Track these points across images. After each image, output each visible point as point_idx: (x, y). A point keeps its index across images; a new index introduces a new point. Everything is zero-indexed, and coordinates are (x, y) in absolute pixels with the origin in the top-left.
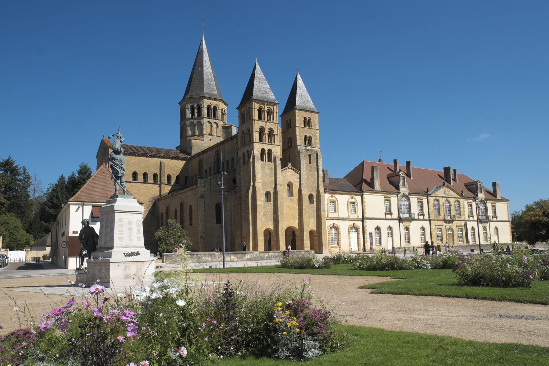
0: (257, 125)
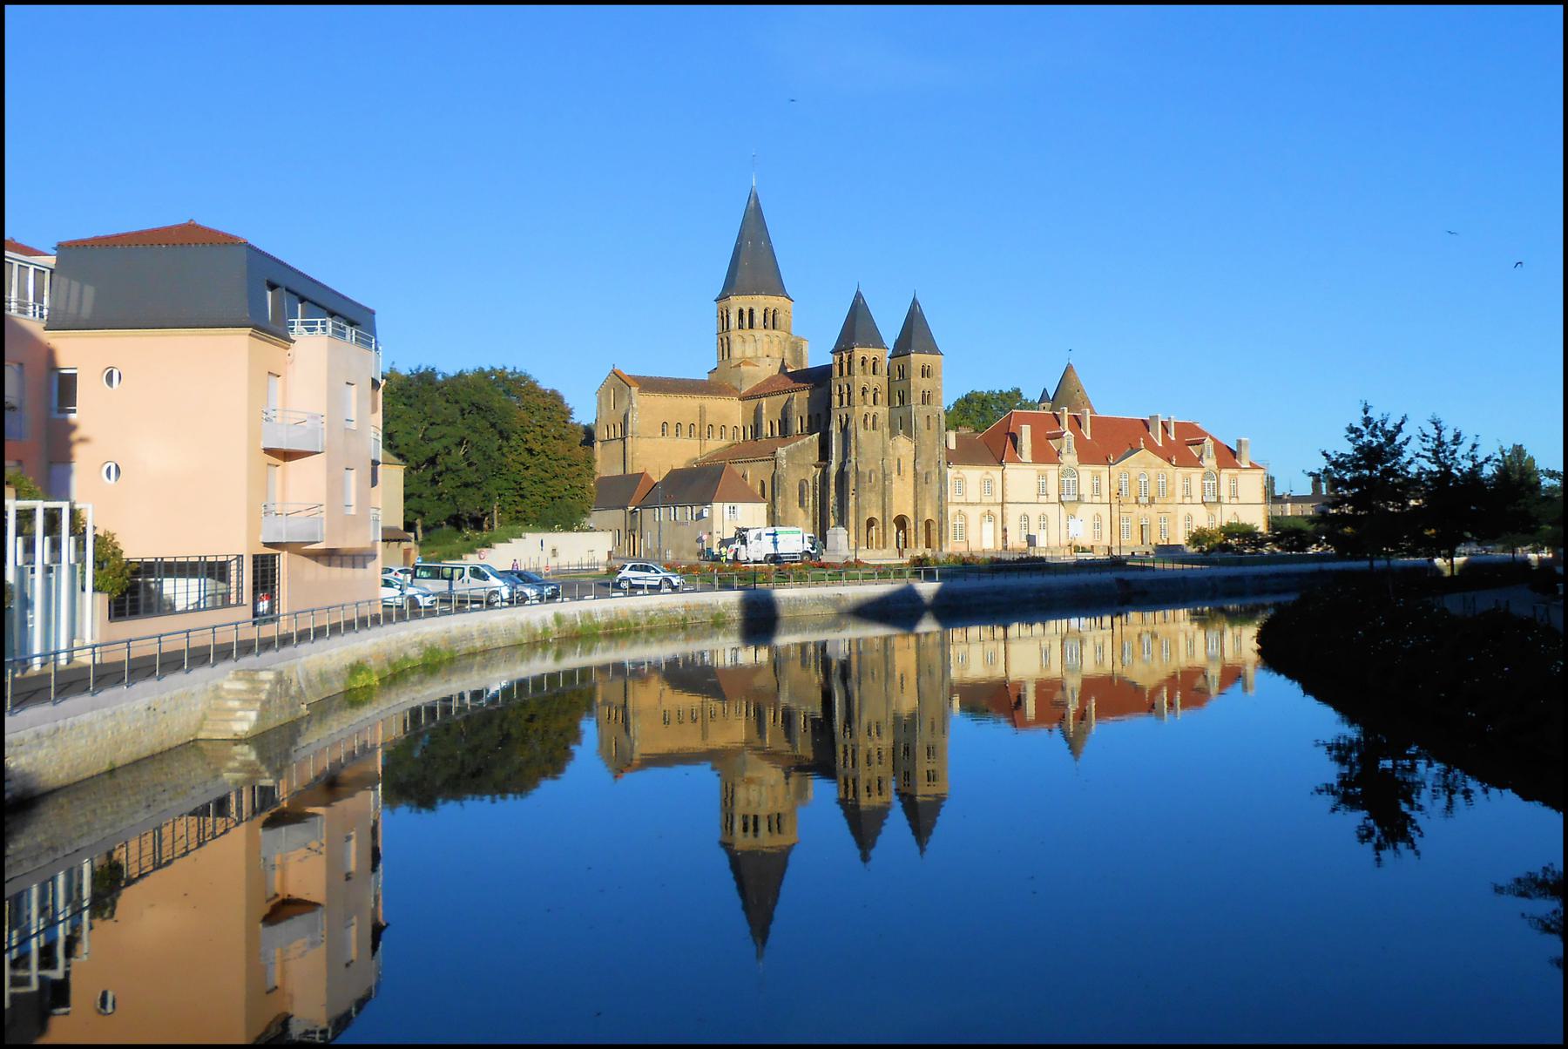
0: (860, 379)
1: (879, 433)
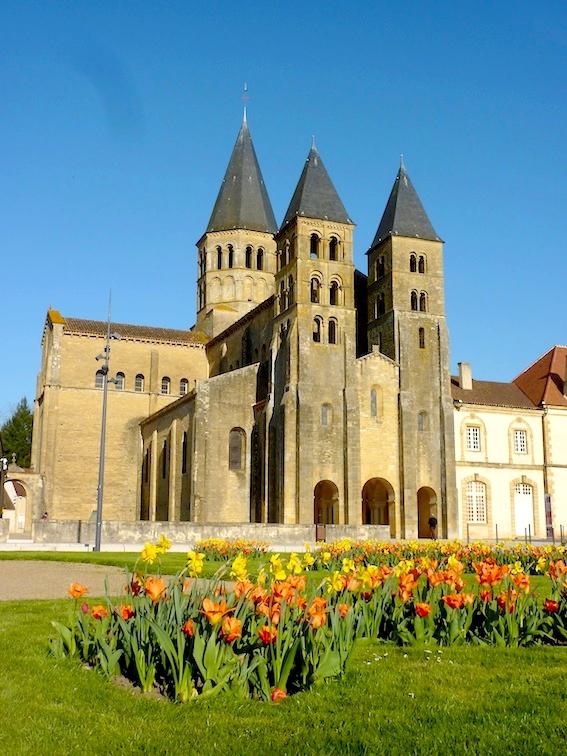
1: (338, 347)
